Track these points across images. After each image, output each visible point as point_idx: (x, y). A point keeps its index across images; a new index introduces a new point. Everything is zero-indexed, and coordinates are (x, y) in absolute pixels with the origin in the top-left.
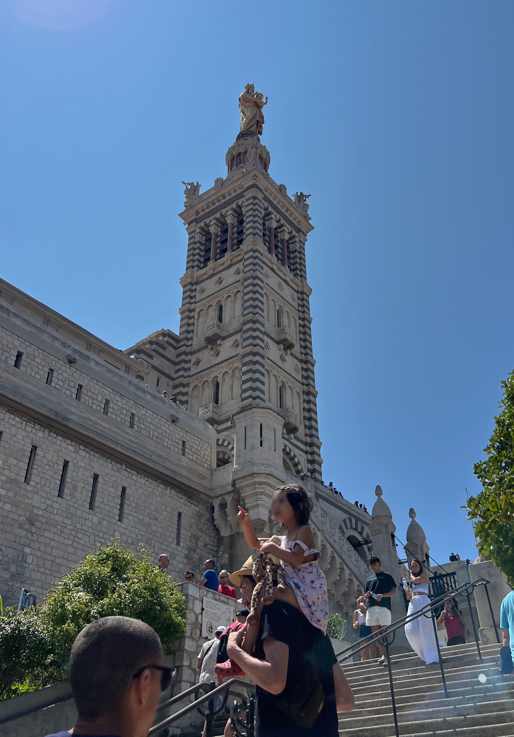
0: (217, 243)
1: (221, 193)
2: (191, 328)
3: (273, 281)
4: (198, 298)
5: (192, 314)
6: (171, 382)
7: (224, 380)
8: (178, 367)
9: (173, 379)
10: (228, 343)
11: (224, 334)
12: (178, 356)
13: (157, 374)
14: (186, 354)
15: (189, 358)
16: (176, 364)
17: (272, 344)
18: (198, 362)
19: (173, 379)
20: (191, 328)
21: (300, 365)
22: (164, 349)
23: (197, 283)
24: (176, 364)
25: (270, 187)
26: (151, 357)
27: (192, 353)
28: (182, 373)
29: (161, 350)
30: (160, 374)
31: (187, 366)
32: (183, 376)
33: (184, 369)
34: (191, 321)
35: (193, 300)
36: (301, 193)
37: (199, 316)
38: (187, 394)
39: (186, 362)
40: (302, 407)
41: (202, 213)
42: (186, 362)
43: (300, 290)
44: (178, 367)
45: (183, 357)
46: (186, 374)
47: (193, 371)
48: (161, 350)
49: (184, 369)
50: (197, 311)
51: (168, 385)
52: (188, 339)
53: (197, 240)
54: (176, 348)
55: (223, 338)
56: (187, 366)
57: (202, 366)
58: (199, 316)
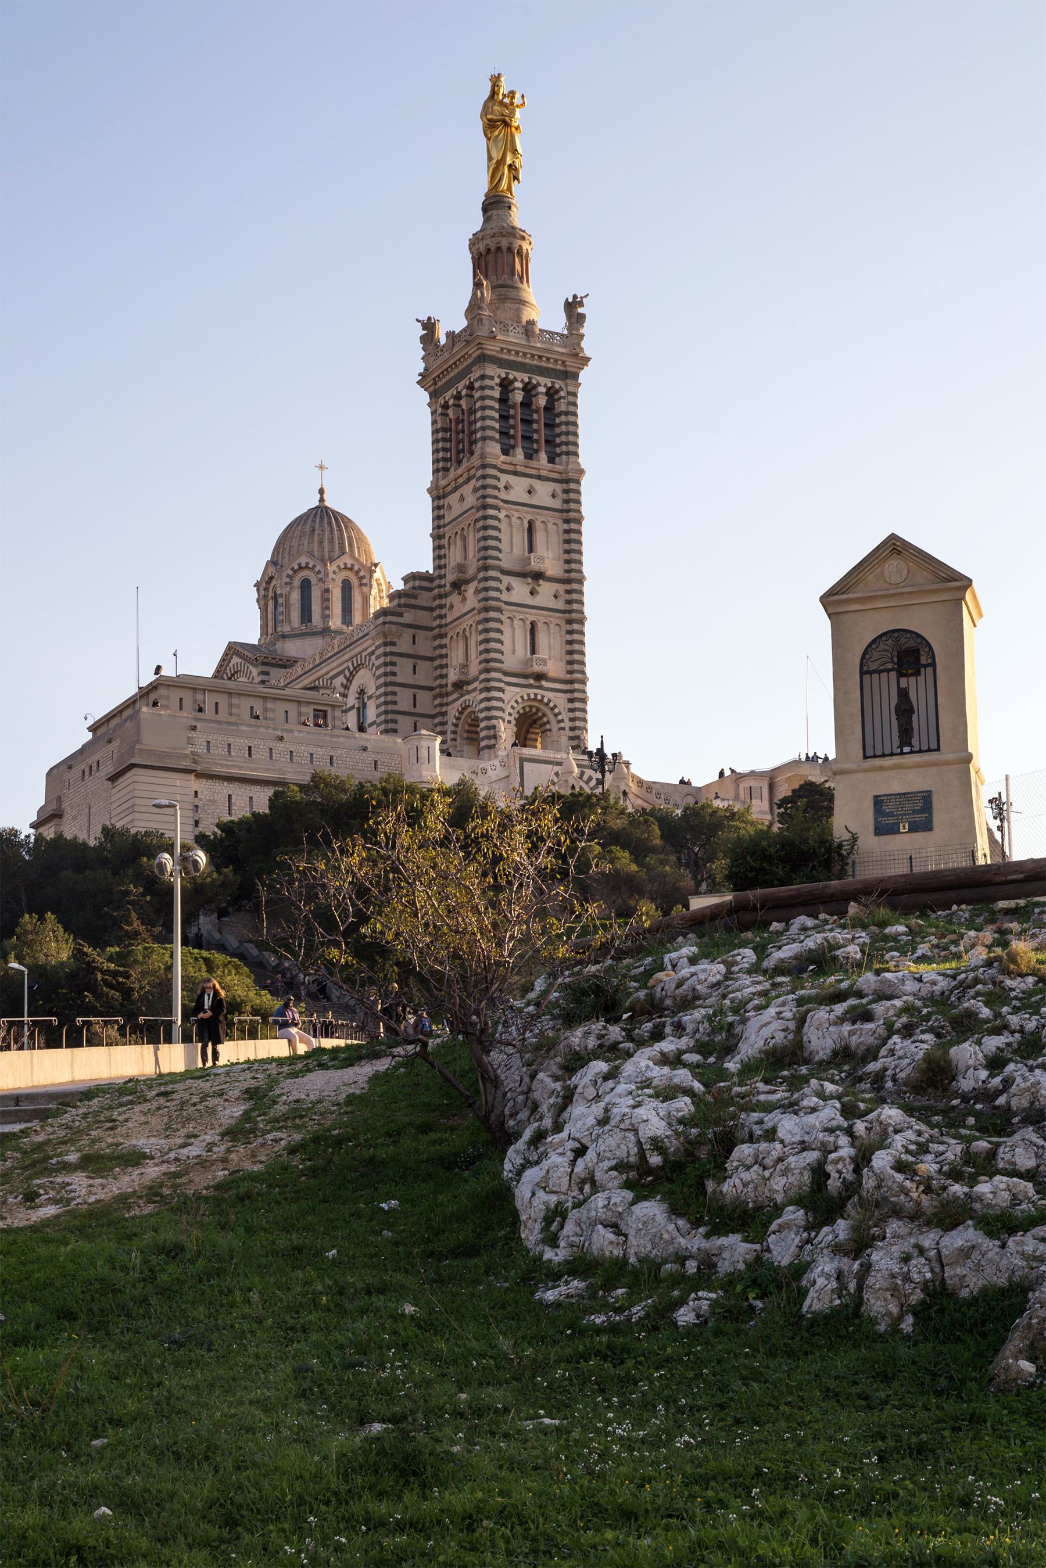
0: (458, 433)
1: (452, 362)
2: (443, 562)
3: (519, 489)
4: (447, 519)
5: (443, 542)
6: (431, 634)
7: (471, 634)
8: (435, 614)
9: (431, 629)
10: (471, 588)
11: (468, 576)
12: (435, 599)
13: (412, 631)
14: (440, 596)
15: (443, 601)
16: (431, 609)
17: (515, 582)
18: (452, 606)
19: (431, 629)
20: (443, 562)
21: (561, 588)
22: (415, 597)
23: (444, 496)
24: (431, 609)
25: (504, 346)
26: (401, 615)
27: (446, 595)
28: (437, 622)
29: (413, 602)
30: (413, 631)
31: (443, 611)
32: (440, 626)
33: (441, 617)
34: (442, 552)
35: (442, 522)
36: (575, 297)
37: (449, 544)
38: (445, 646)
39: (441, 607)
40: (564, 640)
41: (440, 384)
42: (441, 607)
43: (564, 476)
44: (435, 614)
45: (437, 602)
46: (443, 622)
47: (449, 619)
48: (413, 602)
49: (441, 617)
50: (447, 537)
51: (427, 638)
52: (440, 577)
53: (439, 426)
54: (431, 590)
55: (467, 582)
56: (443, 611)
57: (456, 613)
58: (449, 544)
